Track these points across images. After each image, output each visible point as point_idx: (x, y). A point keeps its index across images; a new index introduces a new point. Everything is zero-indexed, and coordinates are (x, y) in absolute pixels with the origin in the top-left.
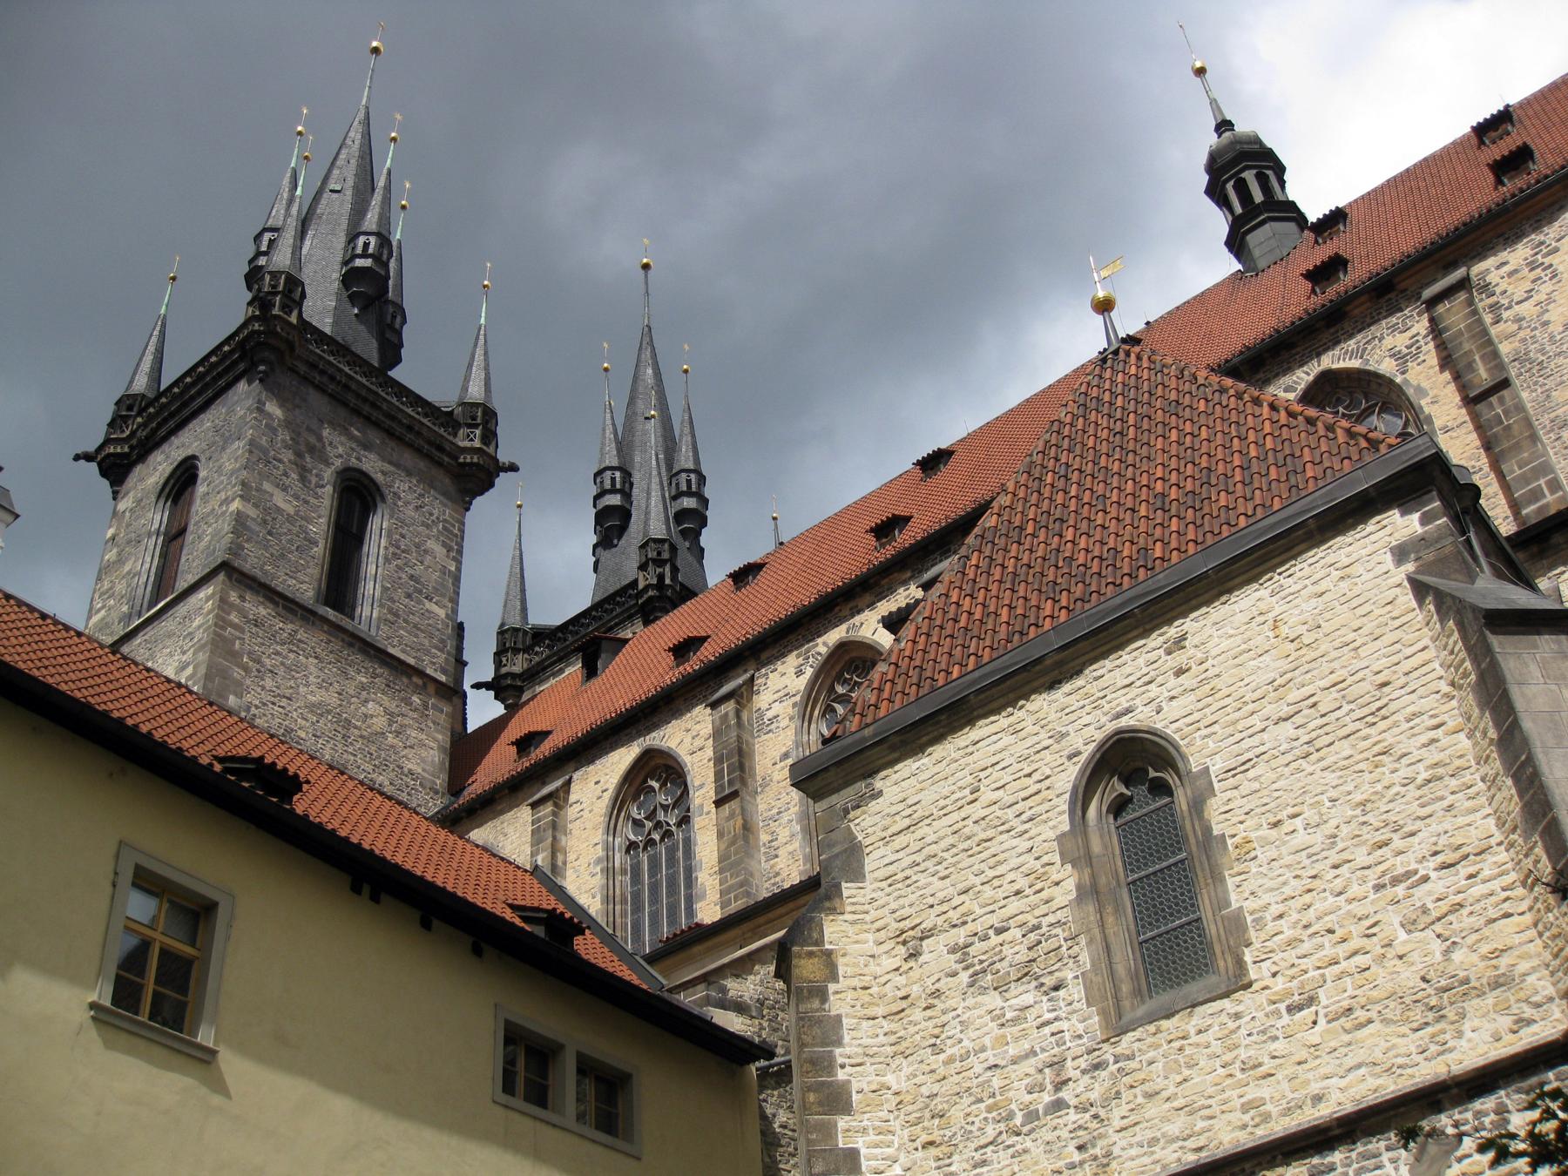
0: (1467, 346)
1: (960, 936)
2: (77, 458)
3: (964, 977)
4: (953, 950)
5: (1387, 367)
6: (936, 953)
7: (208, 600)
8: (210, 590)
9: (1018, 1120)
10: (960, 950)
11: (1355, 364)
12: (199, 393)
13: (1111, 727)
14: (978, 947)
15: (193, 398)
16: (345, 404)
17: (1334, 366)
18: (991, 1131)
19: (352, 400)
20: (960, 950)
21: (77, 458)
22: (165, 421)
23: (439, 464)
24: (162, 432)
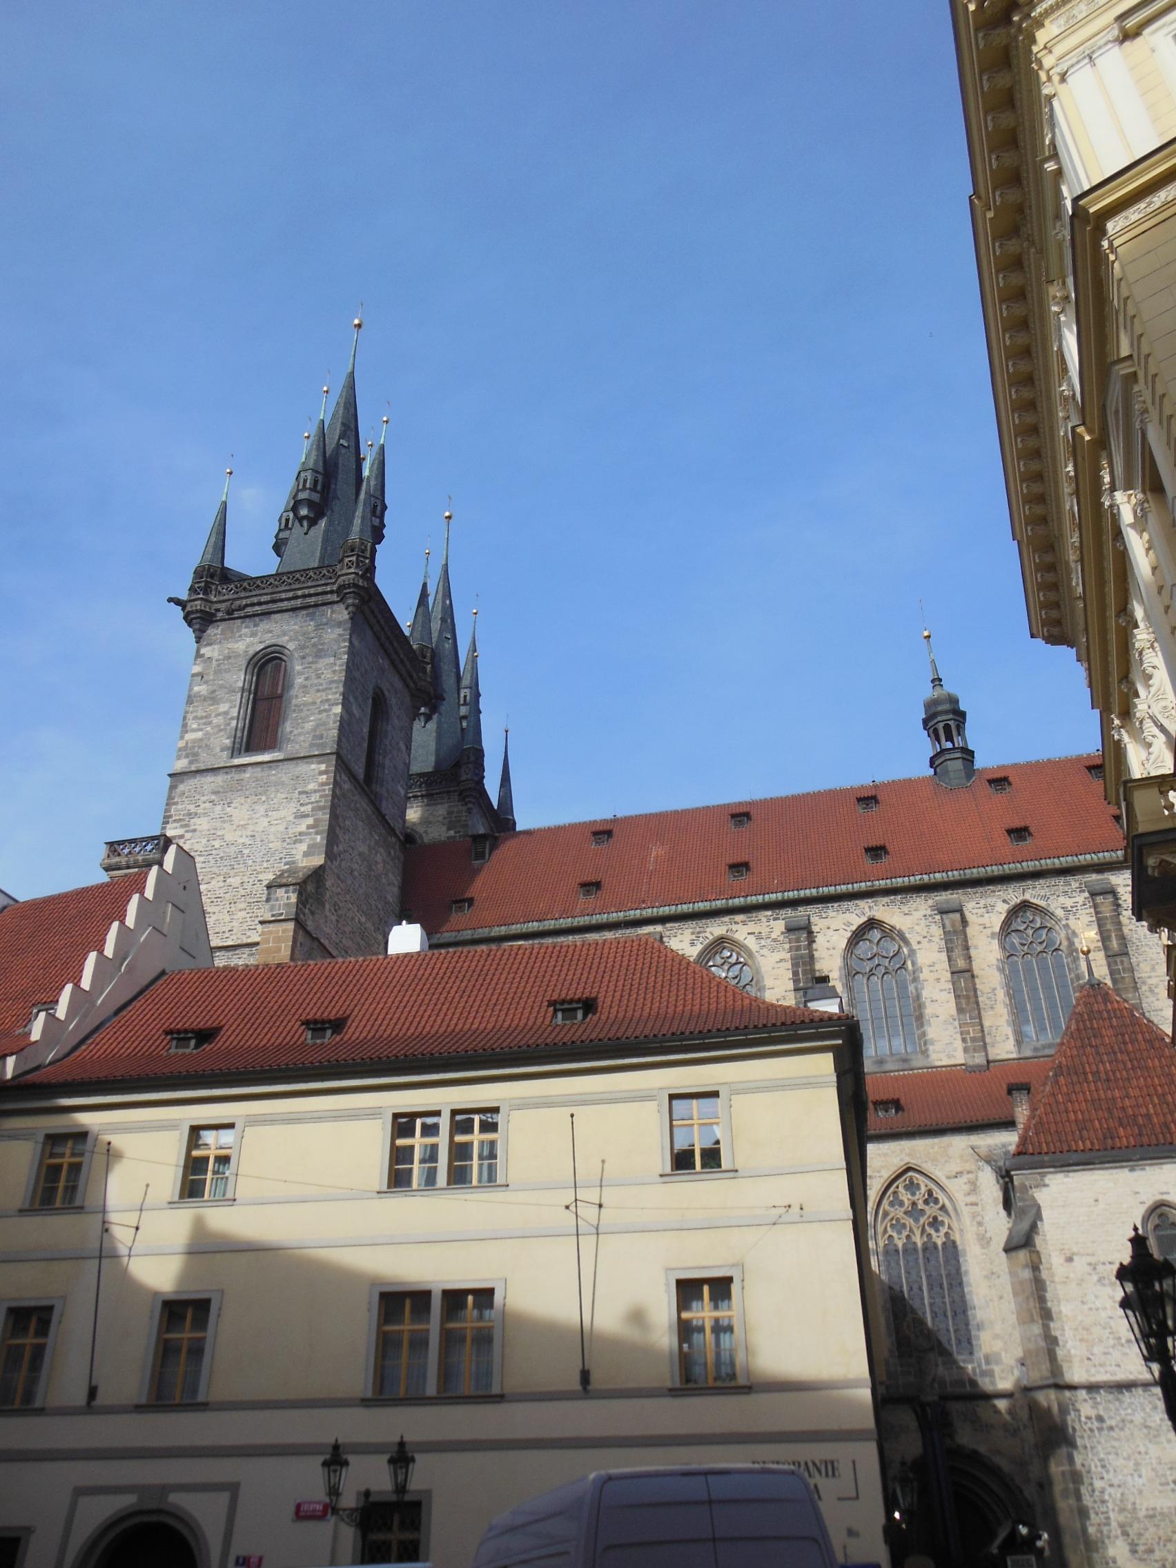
0: (1109, 927)
1: (1093, 1260)
2: (170, 600)
3: (1095, 1278)
4: (1090, 1264)
5: (1059, 913)
6: (1080, 1264)
7: (321, 773)
8: (323, 767)
9: (1123, 1341)
10: (1094, 1266)
11: (1042, 903)
12: (289, 599)
13: (1159, 1197)
14: (1100, 1268)
15: (282, 600)
16: (379, 639)
17: (1032, 900)
18: (1111, 1342)
19: (383, 638)
20: (1094, 1266)
21: (170, 600)
22: (253, 605)
23: (407, 686)
24: (249, 610)
